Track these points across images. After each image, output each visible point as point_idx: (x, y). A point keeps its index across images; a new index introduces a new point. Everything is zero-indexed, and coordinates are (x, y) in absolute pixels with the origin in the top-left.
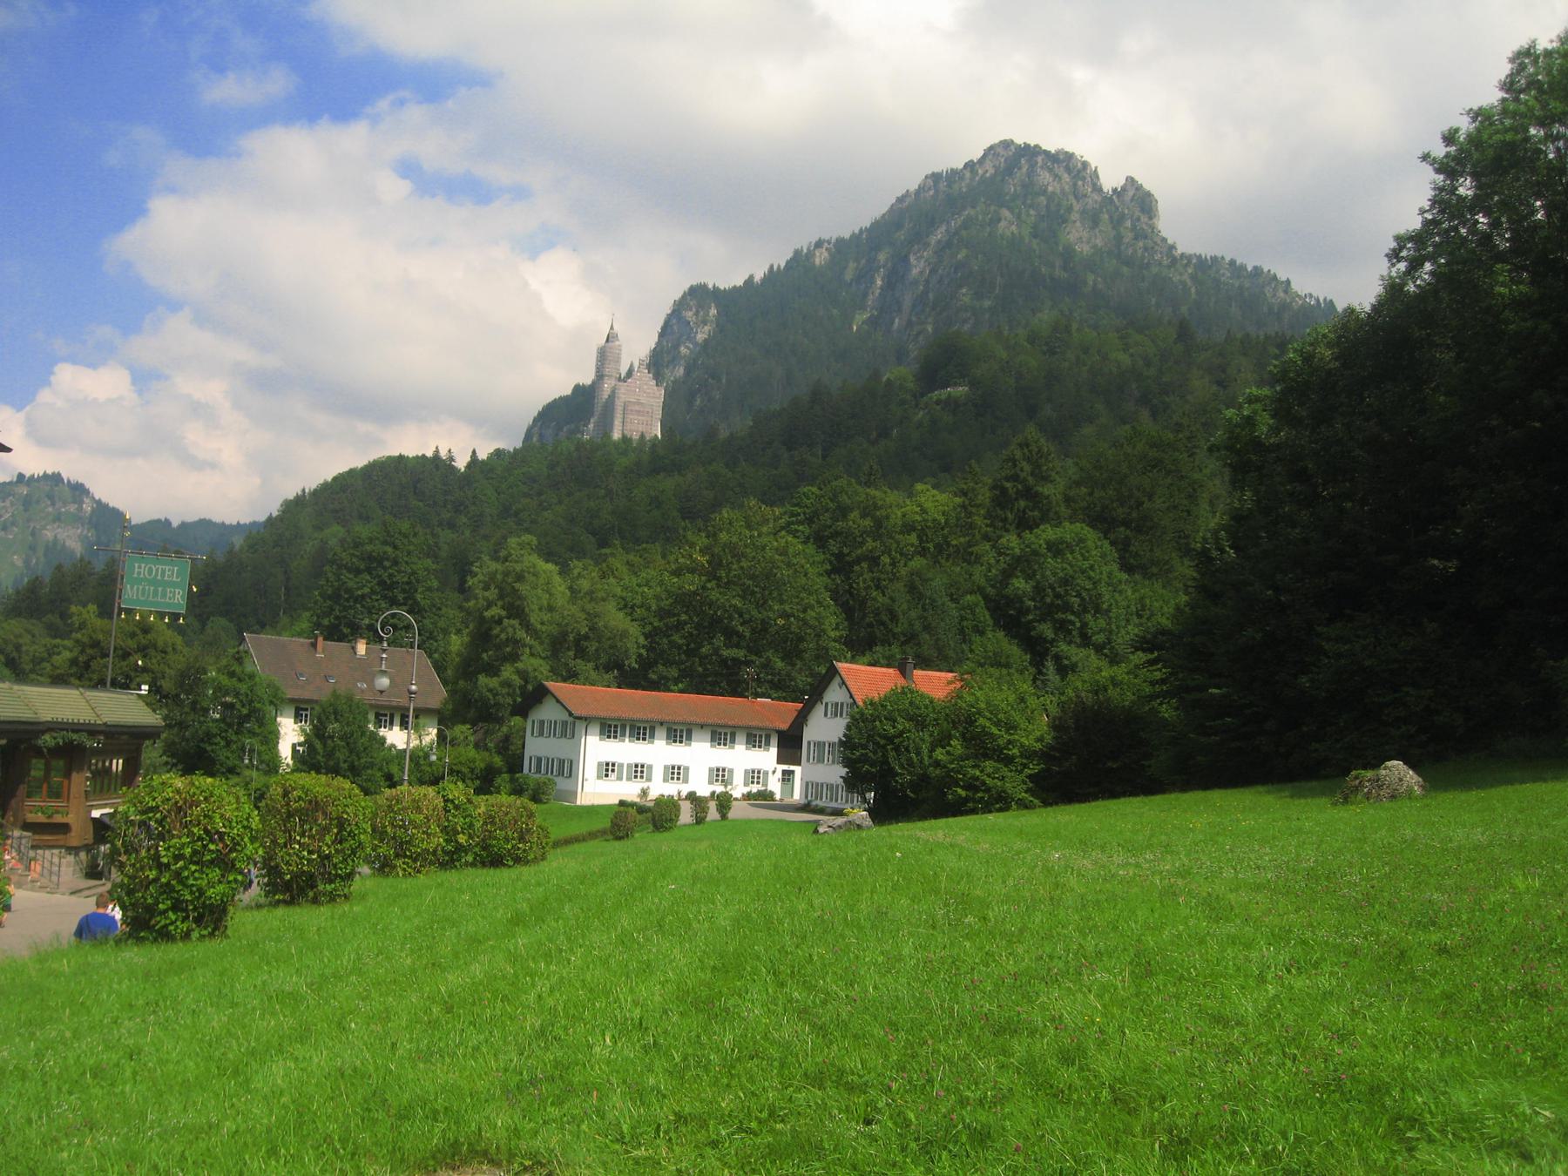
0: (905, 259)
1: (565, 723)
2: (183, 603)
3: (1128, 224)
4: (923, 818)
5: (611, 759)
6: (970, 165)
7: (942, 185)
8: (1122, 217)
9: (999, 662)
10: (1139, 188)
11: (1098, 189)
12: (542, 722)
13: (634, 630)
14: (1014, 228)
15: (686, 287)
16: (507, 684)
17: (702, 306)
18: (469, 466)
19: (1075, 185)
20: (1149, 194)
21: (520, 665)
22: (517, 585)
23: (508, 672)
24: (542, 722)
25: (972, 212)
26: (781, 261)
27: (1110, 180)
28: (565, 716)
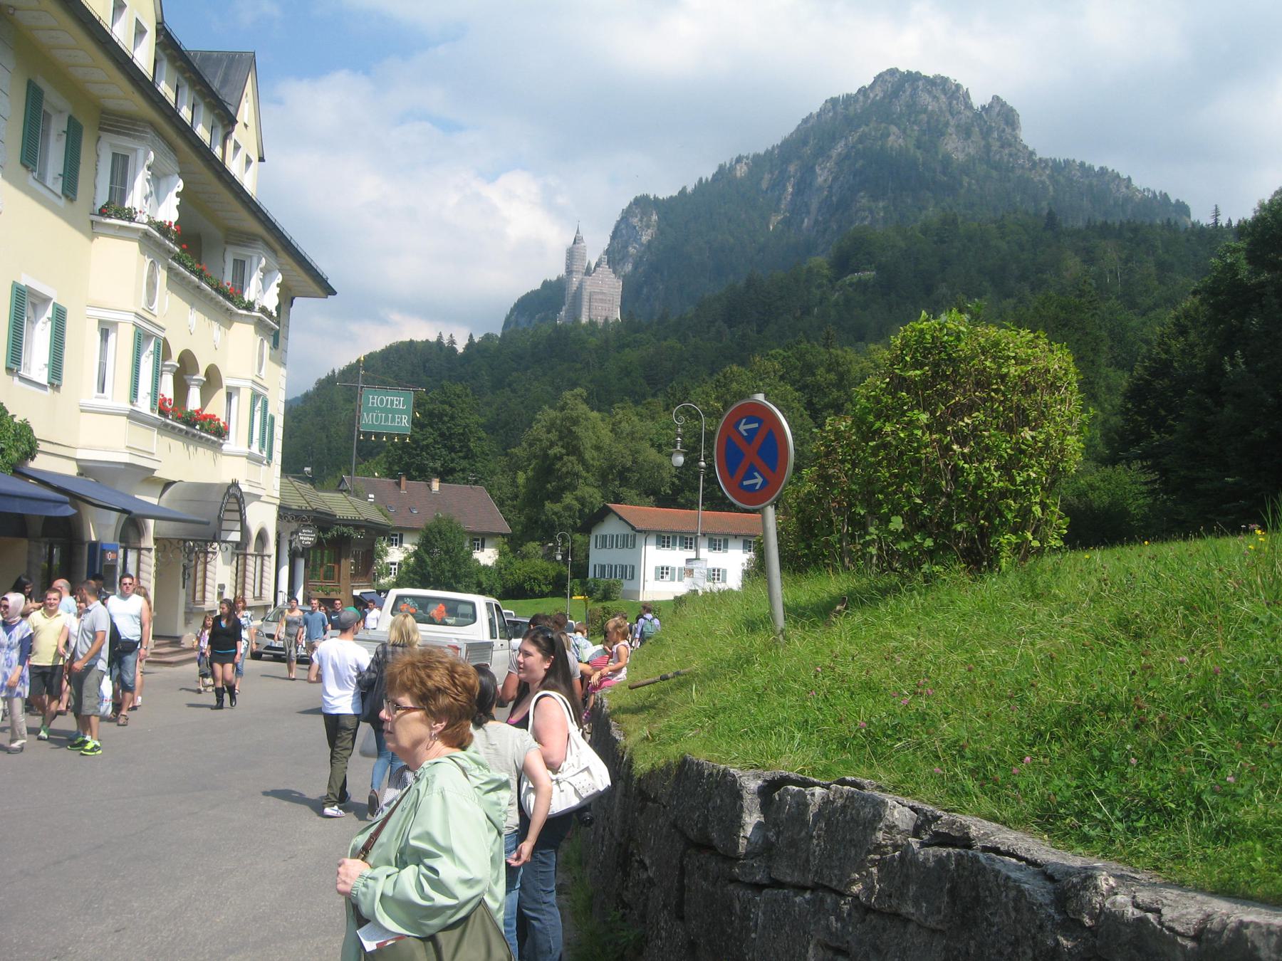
0: (812, 169)
1: (626, 537)
3: (995, 135)
5: (665, 564)
6: (862, 91)
7: (840, 109)
8: (990, 129)
10: (1004, 104)
14: (901, 141)
16: (568, 508)
18: (468, 347)
19: (950, 104)
20: (1012, 110)
21: (578, 493)
22: (574, 429)
23: (568, 498)
24: (604, 537)
25: (867, 129)
27: (979, 99)
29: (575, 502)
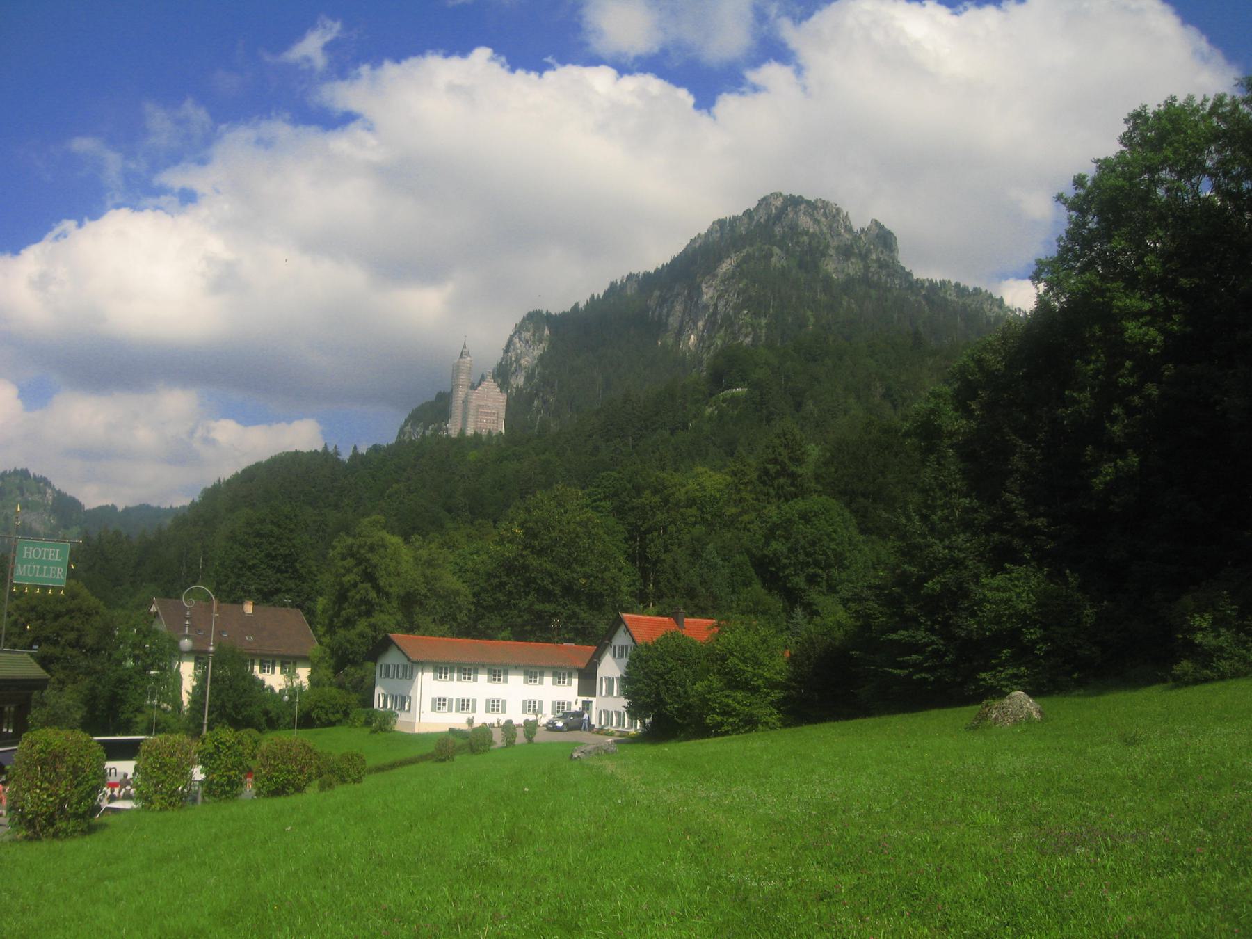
1: (405, 667)
2: (64, 578)
3: (874, 257)
4: (687, 739)
5: (442, 695)
6: (748, 213)
8: (869, 251)
9: (756, 610)
10: (882, 228)
11: (849, 229)
12: (388, 667)
13: (464, 588)
14: (784, 262)
15: (525, 313)
16: (361, 635)
17: (538, 329)
20: (890, 233)
21: (372, 620)
22: (369, 555)
23: (362, 625)
24: (388, 667)
26: (600, 291)
28: (405, 661)
29: (368, 630)
